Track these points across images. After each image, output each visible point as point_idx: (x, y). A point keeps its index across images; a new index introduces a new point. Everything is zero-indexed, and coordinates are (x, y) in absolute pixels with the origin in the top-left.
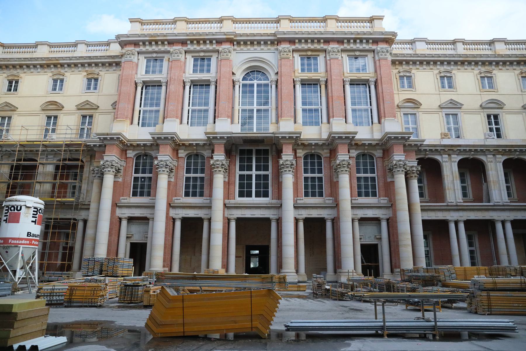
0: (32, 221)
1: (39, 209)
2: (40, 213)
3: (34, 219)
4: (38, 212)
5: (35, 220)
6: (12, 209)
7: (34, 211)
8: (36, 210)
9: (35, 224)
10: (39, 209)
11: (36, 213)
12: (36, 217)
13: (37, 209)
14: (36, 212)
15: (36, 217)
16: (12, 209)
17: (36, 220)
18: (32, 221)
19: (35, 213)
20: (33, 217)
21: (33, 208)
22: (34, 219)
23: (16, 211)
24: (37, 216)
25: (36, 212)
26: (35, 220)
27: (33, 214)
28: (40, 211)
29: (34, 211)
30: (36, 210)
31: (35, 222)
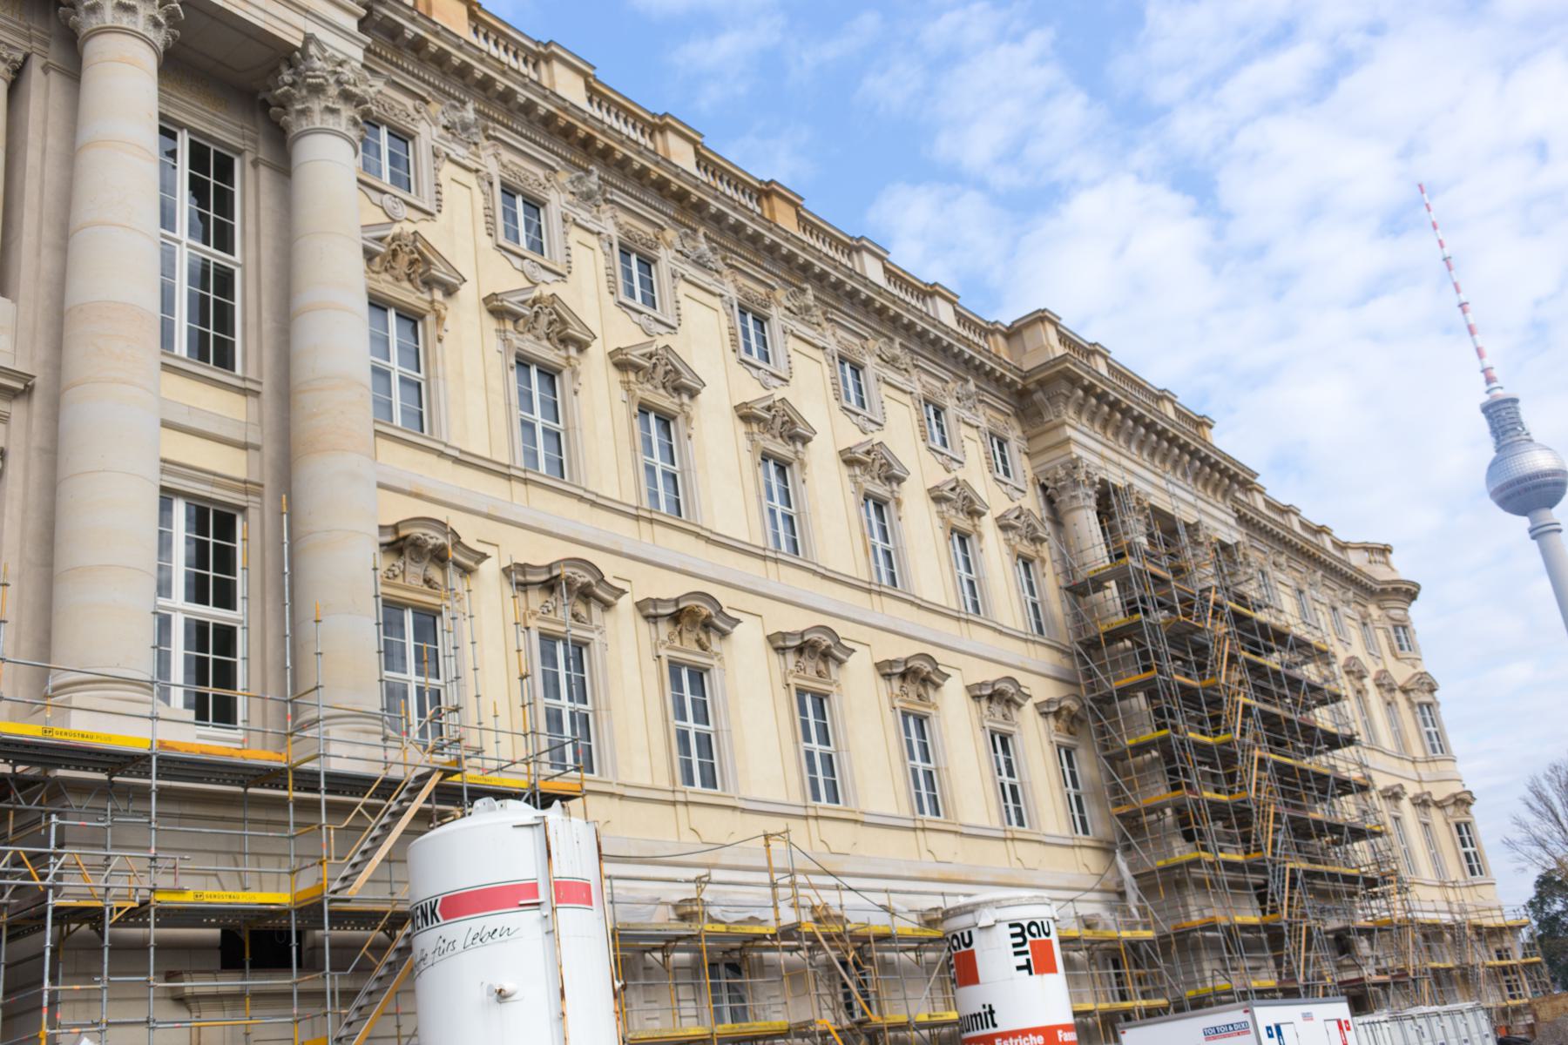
0: (1019, 968)
1: (1025, 924)
2: (1033, 935)
3: (1022, 960)
4: (1027, 934)
5: (1025, 963)
6: (955, 943)
7: (1013, 936)
8: (1018, 930)
9: (1030, 973)
10: (1025, 924)
11: (1020, 940)
12: (1026, 952)
13: (1021, 926)
14: (1022, 935)
15: (1026, 952)
16: (955, 943)
17: (1028, 960)
18: (1019, 968)
19: (1020, 940)
20: (1016, 954)
21: (1006, 925)
22: (1022, 960)
23: (963, 949)
24: (1027, 947)
25: (1022, 935)
26: (1025, 963)
27: (1015, 945)
28: (1034, 929)
29: (1013, 936)
30: (1018, 930)
31: (1027, 967)
